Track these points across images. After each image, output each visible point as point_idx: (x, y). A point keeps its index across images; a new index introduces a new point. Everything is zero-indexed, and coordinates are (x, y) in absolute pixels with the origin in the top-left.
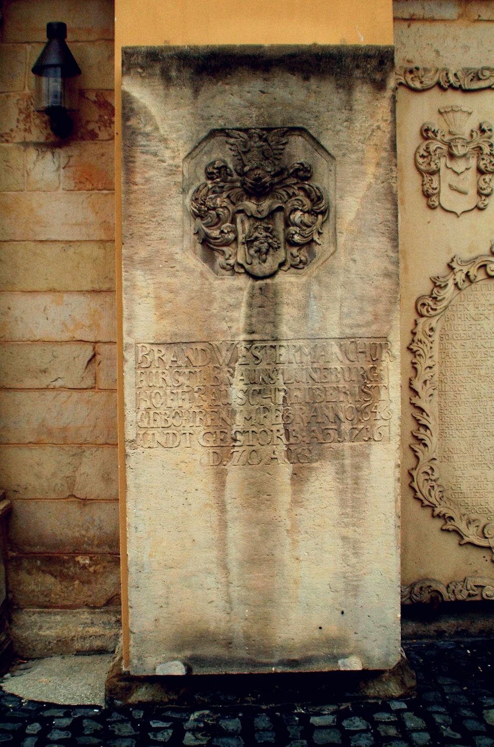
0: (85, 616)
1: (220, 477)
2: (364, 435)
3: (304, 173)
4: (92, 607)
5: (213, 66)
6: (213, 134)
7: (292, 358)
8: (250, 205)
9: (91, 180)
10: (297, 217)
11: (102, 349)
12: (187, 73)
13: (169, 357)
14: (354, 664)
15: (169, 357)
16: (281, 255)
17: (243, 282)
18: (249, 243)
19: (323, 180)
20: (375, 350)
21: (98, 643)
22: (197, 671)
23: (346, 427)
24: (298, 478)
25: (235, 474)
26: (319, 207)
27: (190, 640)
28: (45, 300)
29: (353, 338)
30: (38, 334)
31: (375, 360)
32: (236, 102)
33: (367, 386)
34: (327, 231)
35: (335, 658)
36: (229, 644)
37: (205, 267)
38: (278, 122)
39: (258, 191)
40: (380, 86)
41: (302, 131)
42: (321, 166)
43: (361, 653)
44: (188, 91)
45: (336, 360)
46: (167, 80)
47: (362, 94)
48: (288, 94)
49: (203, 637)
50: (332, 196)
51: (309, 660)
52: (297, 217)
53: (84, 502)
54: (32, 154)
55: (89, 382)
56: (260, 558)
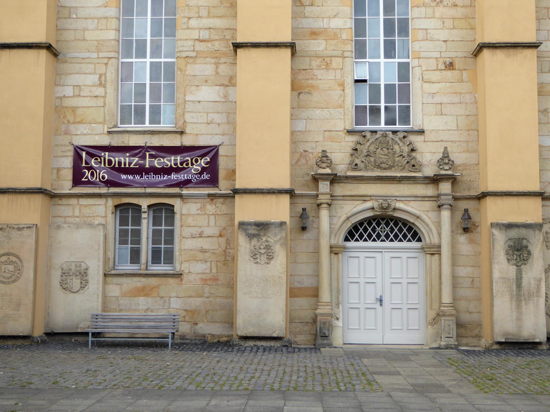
0: (471, 339)
1: (511, 303)
2: (538, 296)
3: (526, 247)
4: (473, 337)
5: (509, 226)
6: (509, 239)
7: (525, 282)
8: (516, 253)
9: (472, 241)
10: (525, 255)
11: (475, 279)
12: (504, 228)
13: (501, 281)
14: (538, 340)
15: (501, 281)
16: (522, 262)
17: (515, 267)
18: (516, 260)
19: (530, 248)
20: (540, 280)
21: (474, 344)
22: (507, 341)
23: (535, 294)
24: (526, 304)
25: (514, 303)
26: (529, 253)
27: (506, 334)
28: (462, 268)
29: (536, 278)
30: (461, 275)
31: (540, 282)
32: (514, 233)
33: (538, 287)
34: (531, 257)
35: (534, 339)
36: (513, 335)
37: (507, 264)
38: (521, 237)
39: (518, 250)
40: (540, 230)
41: (525, 239)
42: (529, 245)
43: (538, 338)
44: (504, 231)
45: (532, 282)
46: (500, 229)
47: (537, 232)
48: (523, 232)
49: (509, 334)
50: (532, 252)
51: (528, 339)
52: (525, 255)
53: (470, 313)
54: (459, 236)
55: (472, 286)
56: (519, 319)
